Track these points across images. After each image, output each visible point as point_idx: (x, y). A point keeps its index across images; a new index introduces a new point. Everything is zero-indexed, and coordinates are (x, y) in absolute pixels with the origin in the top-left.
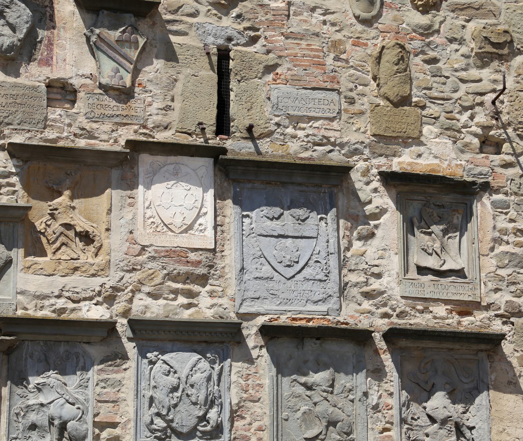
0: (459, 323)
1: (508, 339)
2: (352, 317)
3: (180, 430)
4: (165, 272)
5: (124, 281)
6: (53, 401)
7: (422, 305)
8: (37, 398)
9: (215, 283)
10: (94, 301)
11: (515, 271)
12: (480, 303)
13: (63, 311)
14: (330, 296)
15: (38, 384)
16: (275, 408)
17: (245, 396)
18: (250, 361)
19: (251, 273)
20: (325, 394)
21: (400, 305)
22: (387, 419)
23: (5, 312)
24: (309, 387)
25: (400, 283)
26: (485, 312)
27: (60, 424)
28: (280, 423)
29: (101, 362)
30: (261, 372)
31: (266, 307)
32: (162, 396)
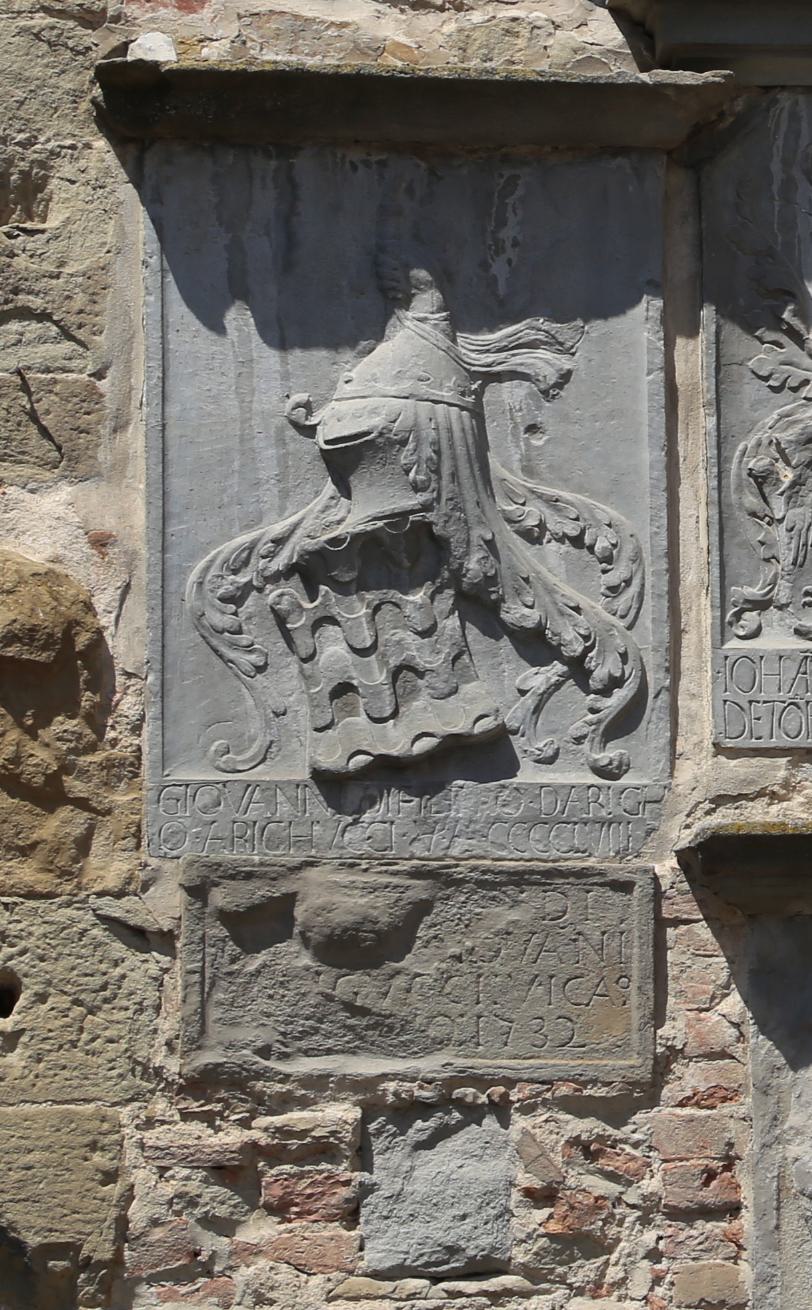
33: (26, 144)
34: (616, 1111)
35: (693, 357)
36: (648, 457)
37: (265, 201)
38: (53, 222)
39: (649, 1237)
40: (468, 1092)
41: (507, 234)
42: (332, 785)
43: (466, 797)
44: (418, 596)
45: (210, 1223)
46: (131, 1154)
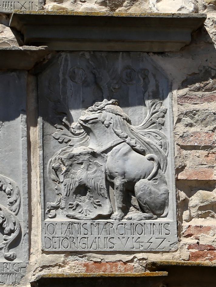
8: (86, 144)
15: (86, 121)
23: (27, 5)
27: (124, 185)
29: (184, 85)
35: (36, 133)
36: (22, 163)
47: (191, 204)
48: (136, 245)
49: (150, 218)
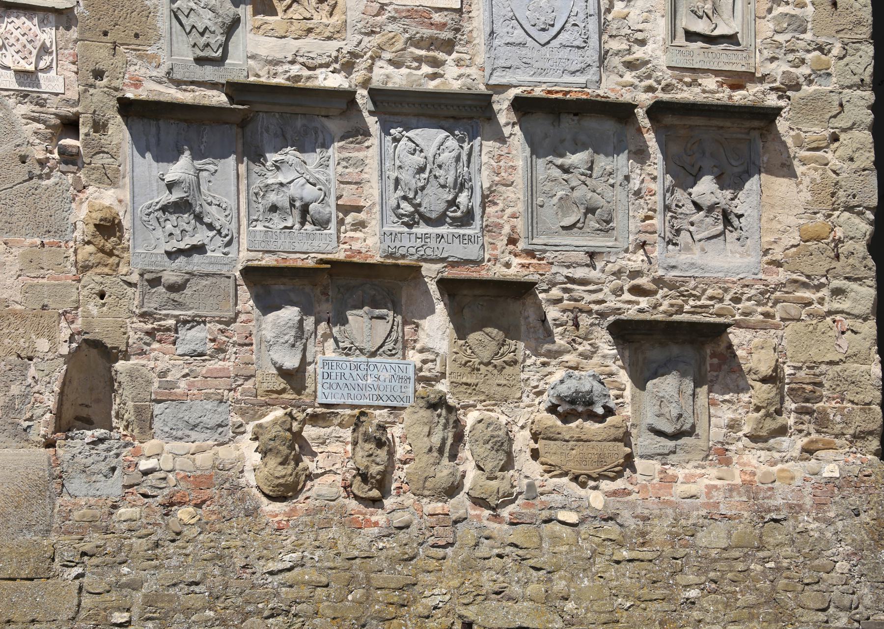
0: (730, 97)
1: (784, 115)
2: (613, 90)
3: (428, 215)
4: (407, 35)
5: (363, 45)
6: (293, 181)
7: (690, 77)
8: (276, 177)
9: (462, 49)
10: (331, 69)
11: (794, 37)
12: (754, 74)
13: (298, 78)
14: (589, 65)
15: (276, 161)
16: (530, 193)
17: (497, 179)
18: (502, 140)
19: (501, 37)
20: (583, 177)
21: (666, 77)
22: (649, 206)
24: (566, 170)
25: (666, 50)
26: (759, 85)
27: (302, 206)
28: (535, 209)
29: (342, 139)
30: (514, 152)
31: (519, 78)
32: (408, 177)
33: (104, 116)
34: (228, 324)
35: (242, 168)
36: (233, 188)
37: (153, 130)
38: (109, 133)
39: (235, 349)
40: (198, 319)
41: (204, 140)
42: (169, 254)
43: (196, 258)
44: (186, 215)
45: (145, 343)
46: (129, 329)
47: (346, 222)
48: (310, 248)
49: (319, 230)
